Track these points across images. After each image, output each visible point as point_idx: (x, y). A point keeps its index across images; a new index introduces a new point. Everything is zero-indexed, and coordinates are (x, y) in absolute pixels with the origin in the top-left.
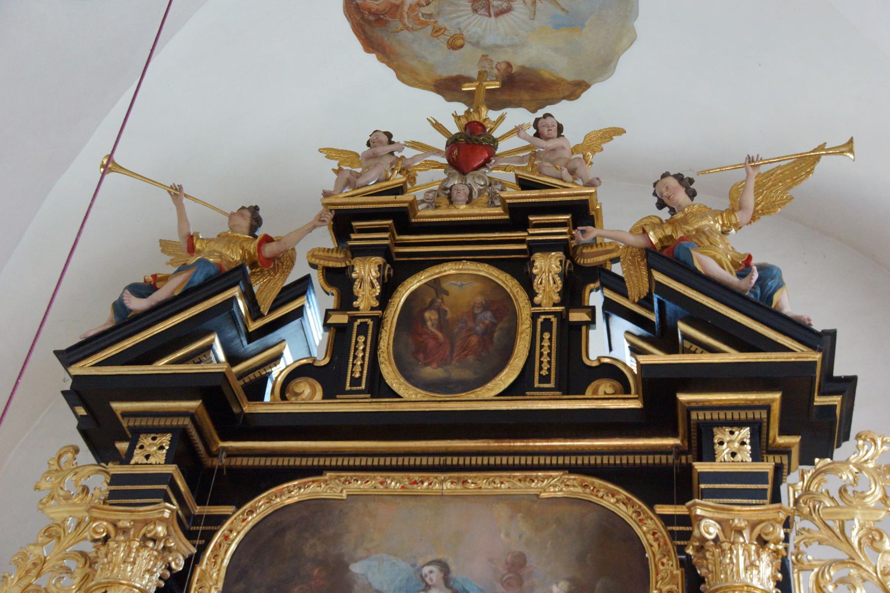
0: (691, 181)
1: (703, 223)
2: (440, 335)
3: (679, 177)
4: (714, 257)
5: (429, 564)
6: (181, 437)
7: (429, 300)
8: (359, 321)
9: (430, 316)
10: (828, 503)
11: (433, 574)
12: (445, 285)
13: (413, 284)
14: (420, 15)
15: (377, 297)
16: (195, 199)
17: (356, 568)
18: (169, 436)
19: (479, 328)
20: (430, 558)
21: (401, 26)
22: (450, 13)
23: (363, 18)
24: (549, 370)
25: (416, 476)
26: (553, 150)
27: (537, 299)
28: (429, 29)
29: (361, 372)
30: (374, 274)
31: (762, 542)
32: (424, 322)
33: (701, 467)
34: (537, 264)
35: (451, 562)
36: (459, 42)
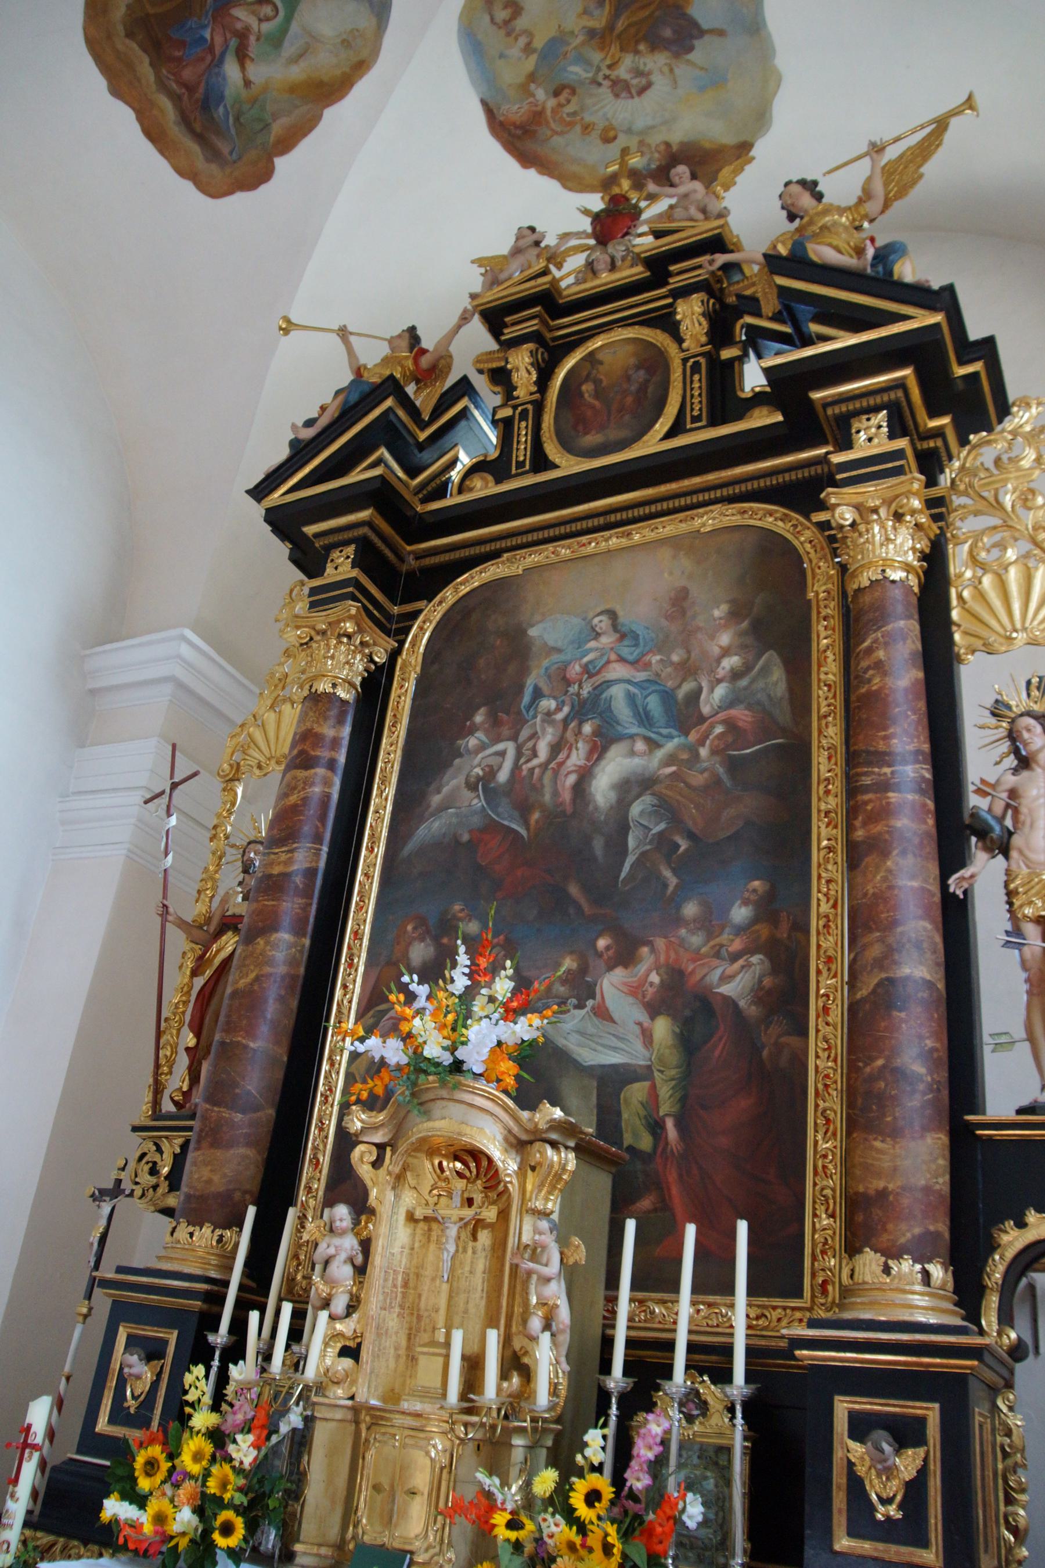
0: (815, 183)
1: (827, 219)
2: (597, 403)
3: (803, 183)
4: (830, 245)
5: (598, 615)
7: (585, 373)
8: (520, 408)
9: (587, 388)
11: (602, 623)
12: (600, 356)
13: (570, 363)
14: (565, 116)
15: (535, 383)
16: (358, 334)
17: (533, 632)
18: (353, 547)
19: (633, 388)
20: (599, 610)
21: (549, 133)
22: (594, 105)
23: (510, 134)
24: (700, 409)
25: (584, 539)
27: (685, 345)
28: (578, 128)
29: (525, 455)
30: (527, 360)
31: (898, 517)
32: (581, 395)
34: (679, 310)
36: (612, 134)
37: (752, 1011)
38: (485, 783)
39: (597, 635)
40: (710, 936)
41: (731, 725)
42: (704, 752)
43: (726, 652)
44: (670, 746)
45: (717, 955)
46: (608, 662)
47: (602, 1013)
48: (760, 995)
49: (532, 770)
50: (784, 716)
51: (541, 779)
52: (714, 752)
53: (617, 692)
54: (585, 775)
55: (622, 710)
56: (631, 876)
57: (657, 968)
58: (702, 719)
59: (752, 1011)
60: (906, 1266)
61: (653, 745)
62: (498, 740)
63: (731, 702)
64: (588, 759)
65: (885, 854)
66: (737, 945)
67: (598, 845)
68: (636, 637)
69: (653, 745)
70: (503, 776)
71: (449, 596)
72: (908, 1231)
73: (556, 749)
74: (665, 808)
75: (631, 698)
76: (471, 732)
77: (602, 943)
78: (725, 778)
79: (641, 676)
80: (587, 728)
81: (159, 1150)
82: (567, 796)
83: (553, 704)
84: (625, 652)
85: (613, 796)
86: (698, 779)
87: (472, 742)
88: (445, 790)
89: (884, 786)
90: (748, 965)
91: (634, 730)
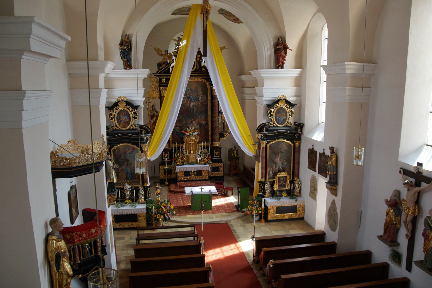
11: (189, 89)
37: (204, 125)
39: (189, 90)
41: (202, 101)
42: (200, 104)
44: (197, 103)
45: (202, 120)
46: (190, 93)
53: (192, 97)
54: (190, 105)
58: (199, 101)
59: (204, 125)
60: (217, 143)
61: (195, 102)
63: (201, 99)
66: (203, 120)
67: (191, 111)
68: (193, 91)
69: (195, 102)
72: (217, 141)
73: (186, 101)
74: (197, 108)
77: (193, 119)
79: (194, 95)
82: (188, 106)
84: (192, 92)
85: (192, 107)
86: (199, 106)
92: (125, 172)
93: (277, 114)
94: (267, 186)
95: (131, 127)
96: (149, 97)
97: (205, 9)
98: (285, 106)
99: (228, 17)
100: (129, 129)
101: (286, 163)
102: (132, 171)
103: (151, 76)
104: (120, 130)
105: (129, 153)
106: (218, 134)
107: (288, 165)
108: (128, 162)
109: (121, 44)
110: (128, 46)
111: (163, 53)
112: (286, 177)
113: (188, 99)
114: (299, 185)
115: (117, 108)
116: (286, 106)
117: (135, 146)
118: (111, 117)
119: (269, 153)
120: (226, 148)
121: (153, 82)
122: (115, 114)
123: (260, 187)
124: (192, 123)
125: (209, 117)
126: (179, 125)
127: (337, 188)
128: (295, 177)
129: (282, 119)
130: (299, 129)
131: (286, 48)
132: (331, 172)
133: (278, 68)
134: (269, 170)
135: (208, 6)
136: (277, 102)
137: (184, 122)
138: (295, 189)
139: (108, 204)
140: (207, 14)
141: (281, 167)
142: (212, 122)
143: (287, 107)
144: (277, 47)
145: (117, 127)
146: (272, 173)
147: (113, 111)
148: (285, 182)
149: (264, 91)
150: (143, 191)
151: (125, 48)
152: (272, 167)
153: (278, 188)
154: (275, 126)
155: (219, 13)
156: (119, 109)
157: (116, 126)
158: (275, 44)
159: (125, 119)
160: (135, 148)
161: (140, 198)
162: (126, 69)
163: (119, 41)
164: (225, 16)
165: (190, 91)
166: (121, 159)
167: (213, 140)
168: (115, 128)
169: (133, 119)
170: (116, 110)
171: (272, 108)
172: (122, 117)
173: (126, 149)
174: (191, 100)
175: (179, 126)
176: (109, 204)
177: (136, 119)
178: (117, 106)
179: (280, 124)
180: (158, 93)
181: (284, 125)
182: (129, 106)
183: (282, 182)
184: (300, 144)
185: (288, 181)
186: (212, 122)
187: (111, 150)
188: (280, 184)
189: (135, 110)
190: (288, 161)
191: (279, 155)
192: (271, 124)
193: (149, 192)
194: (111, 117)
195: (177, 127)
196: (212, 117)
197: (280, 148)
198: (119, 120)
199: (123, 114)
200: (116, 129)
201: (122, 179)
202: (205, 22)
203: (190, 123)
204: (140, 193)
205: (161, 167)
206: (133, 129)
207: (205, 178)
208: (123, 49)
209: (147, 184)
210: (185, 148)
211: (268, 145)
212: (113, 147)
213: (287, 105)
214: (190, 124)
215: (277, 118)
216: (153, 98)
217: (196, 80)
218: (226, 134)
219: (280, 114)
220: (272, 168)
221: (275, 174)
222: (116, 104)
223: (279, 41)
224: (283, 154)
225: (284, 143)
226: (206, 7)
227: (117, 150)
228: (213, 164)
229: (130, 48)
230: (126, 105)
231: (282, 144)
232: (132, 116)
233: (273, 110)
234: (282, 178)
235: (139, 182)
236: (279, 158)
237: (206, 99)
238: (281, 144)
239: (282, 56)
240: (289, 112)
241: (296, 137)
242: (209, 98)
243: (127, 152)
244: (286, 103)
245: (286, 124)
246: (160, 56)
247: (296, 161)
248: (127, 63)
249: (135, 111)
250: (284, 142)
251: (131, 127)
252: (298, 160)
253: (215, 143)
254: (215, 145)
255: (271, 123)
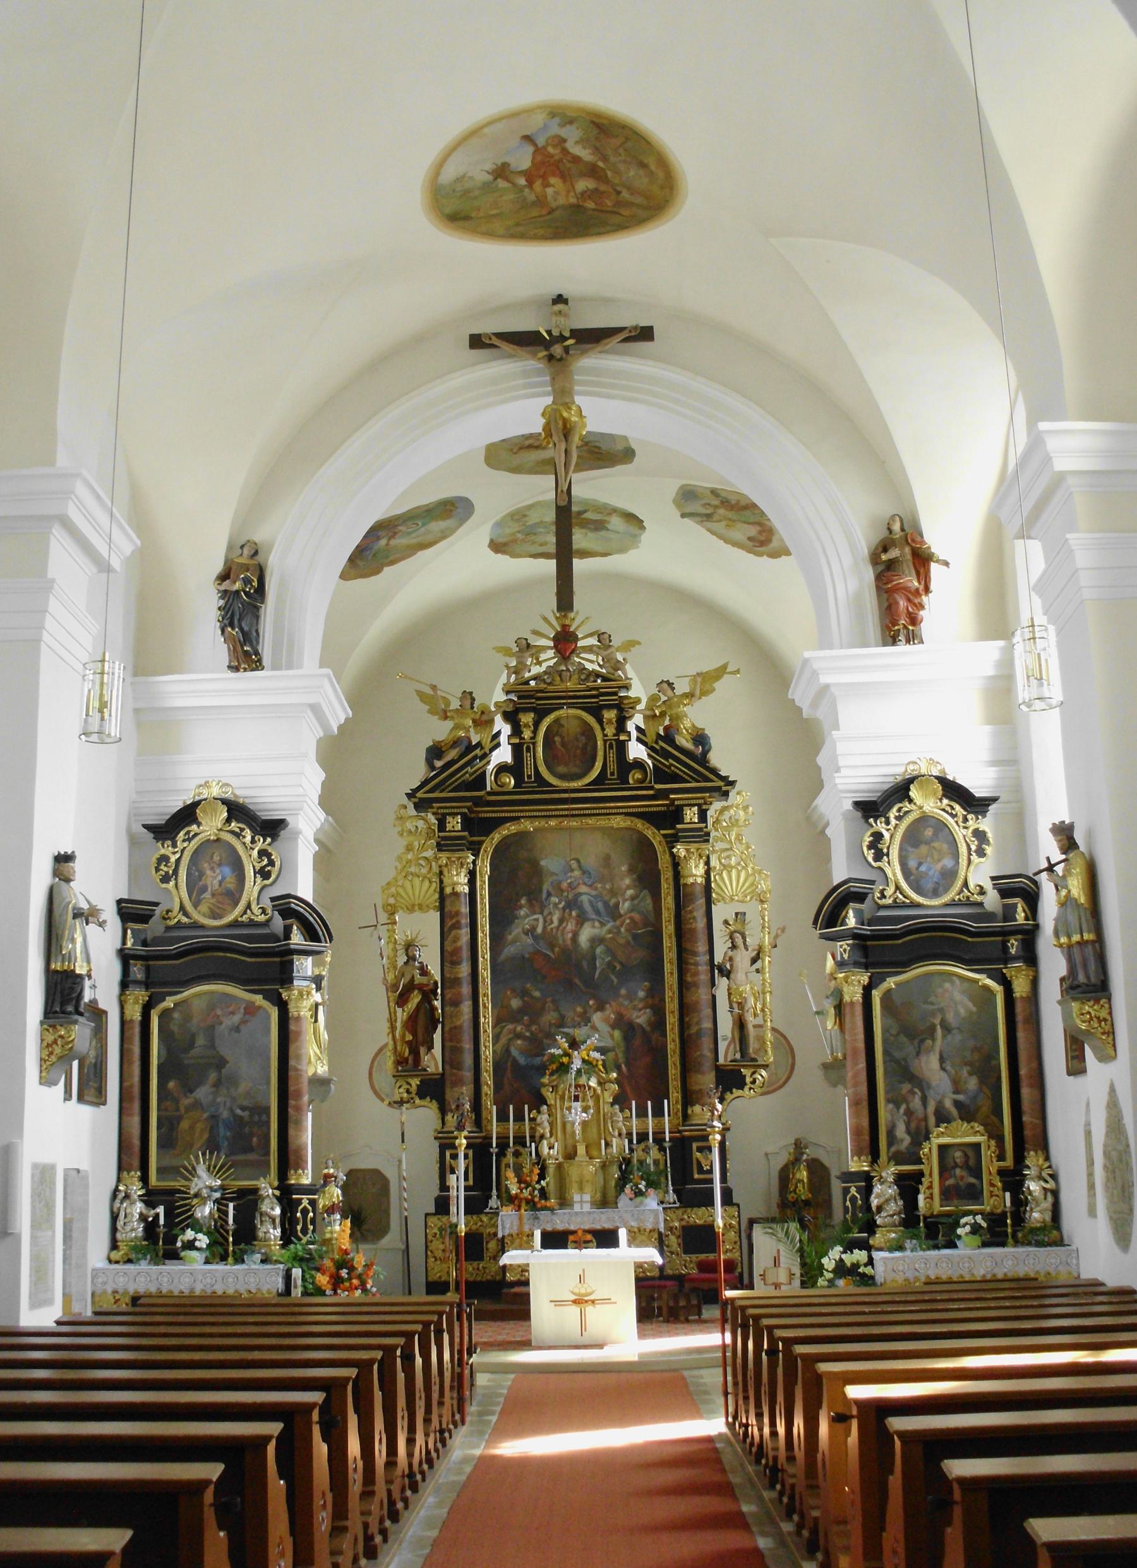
6: (463, 815)
9: (557, 739)
10: (725, 824)
11: (574, 864)
12: (563, 722)
17: (543, 863)
19: (580, 745)
25: (561, 819)
26: (608, 655)
31: (700, 856)
32: (554, 742)
33: (678, 826)
35: (580, 858)
37: (648, 1029)
38: (531, 932)
39: (572, 870)
40: (631, 1002)
41: (631, 918)
42: (623, 930)
43: (628, 888)
44: (609, 925)
45: (634, 1009)
46: (579, 884)
47: (594, 1028)
48: (650, 1023)
49: (552, 929)
50: (652, 918)
51: (556, 933)
52: (627, 930)
53: (584, 899)
55: (587, 907)
56: (599, 977)
57: (614, 1013)
58: (620, 916)
59: (648, 1029)
61: (602, 924)
62: (535, 913)
63: (631, 910)
64: (576, 927)
65: (698, 988)
66: (641, 1005)
67: (585, 964)
69: (602, 924)
70: (539, 930)
71: (496, 837)
73: (561, 921)
74: (609, 951)
75: (590, 902)
76: (521, 907)
77: (591, 1002)
78: (632, 942)
79: (594, 893)
80: (574, 913)
81: (409, 1084)
82: (569, 942)
83: (557, 900)
84: (586, 880)
85: (588, 944)
86: (622, 941)
87: (522, 912)
88: (513, 934)
89: (696, 964)
90: (645, 1013)
91: (594, 917)
92: (206, 1115)
93: (910, 849)
94: (884, 1192)
95: (245, 913)
96: (389, 905)
97: (561, 423)
98: (944, 810)
99: (720, 527)
100: (235, 924)
101: (972, 1083)
102: (239, 1112)
103: (402, 811)
104: (196, 926)
105: (231, 1030)
106: (708, 1064)
107: (985, 1089)
108: (223, 1071)
109: (224, 577)
110: (247, 581)
111: (455, 704)
112: (977, 1147)
113: (571, 911)
114: (1047, 1186)
115: (192, 834)
116: (948, 809)
117: (258, 999)
118: (165, 869)
119: (885, 1031)
120: (768, 1160)
121: (411, 838)
122: (183, 859)
123: (848, 1203)
124: (587, 1020)
125: (668, 994)
126: (528, 1030)
127: (1110, 1013)
128: (1026, 1154)
129: (932, 870)
130: (1020, 909)
131: (922, 560)
132: (1069, 937)
133: (894, 641)
134: (892, 1115)
135: (570, 408)
136: (901, 791)
137: (550, 1017)
138: (1028, 1208)
139: (41, 1066)
140: (566, 441)
141: (948, 1104)
142: (685, 1009)
143: (953, 816)
144: (884, 557)
145: (186, 914)
146: (908, 1132)
147: (174, 845)
148: (977, 1172)
149: (841, 748)
150: (275, 1201)
151: (238, 586)
152: (905, 1100)
153: (941, 1206)
154: (904, 902)
155: (683, 516)
156: (200, 836)
157: (182, 908)
158: (876, 548)
159: (223, 878)
160: (257, 1004)
161: (261, 1234)
162: (236, 669)
163: (219, 567)
164: (709, 524)
165: (577, 873)
166: (193, 1053)
167: (689, 1098)
168: (176, 920)
169: (255, 877)
170: (184, 841)
171: (883, 819)
172: (208, 872)
173: (219, 1012)
174: (580, 907)
175: (528, 1034)
176: (44, 1067)
177: (268, 878)
178: (189, 824)
179: (930, 894)
180: (434, 885)
181: (946, 899)
182: (239, 825)
183: (958, 1171)
184: (1035, 983)
185: (990, 1165)
186: (685, 1009)
187: (152, 1011)
188: (950, 1182)
189: (264, 841)
190: (986, 1071)
191: (934, 1040)
192: (883, 896)
193: (311, 1214)
194: (165, 869)
195: (519, 1042)
196: (683, 986)
197: (936, 1007)
198: (195, 887)
199: (216, 858)
200: (179, 921)
201: (191, 1146)
202: (563, 473)
203: (577, 1019)
204: (261, 1214)
205: (433, 1221)
206: (252, 924)
207: (644, 1272)
208: (231, 592)
209: (300, 1171)
210: (548, 1130)
211: (876, 995)
212: (164, 1000)
213: (953, 804)
214: (579, 1025)
215: (912, 864)
216: (411, 909)
217: (603, 822)
218: (754, 1073)
219: (924, 849)
220: (903, 1107)
221: (920, 1135)
222: (187, 815)
223: (890, 531)
224: (956, 1038)
225: (953, 983)
226: (565, 414)
227: (176, 1015)
228: (689, 1210)
229: (256, 591)
230: (228, 821)
231: (947, 985)
232: (254, 867)
233: (888, 830)
234: (958, 1154)
235: (269, 1161)
236: (938, 1056)
237: (650, 907)
238: (941, 986)
239: (906, 589)
240: (964, 836)
241: (1013, 951)
242: (668, 901)
243: (221, 1023)
244: (945, 795)
245: (959, 894)
246: (439, 719)
247: (1023, 1072)
248: (242, 648)
249: (265, 846)
250: (955, 978)
251: (245, 913)
252: (1034, 1065)
253: (697, 1108)
254: (694, 1122)
255: (882, 892)
